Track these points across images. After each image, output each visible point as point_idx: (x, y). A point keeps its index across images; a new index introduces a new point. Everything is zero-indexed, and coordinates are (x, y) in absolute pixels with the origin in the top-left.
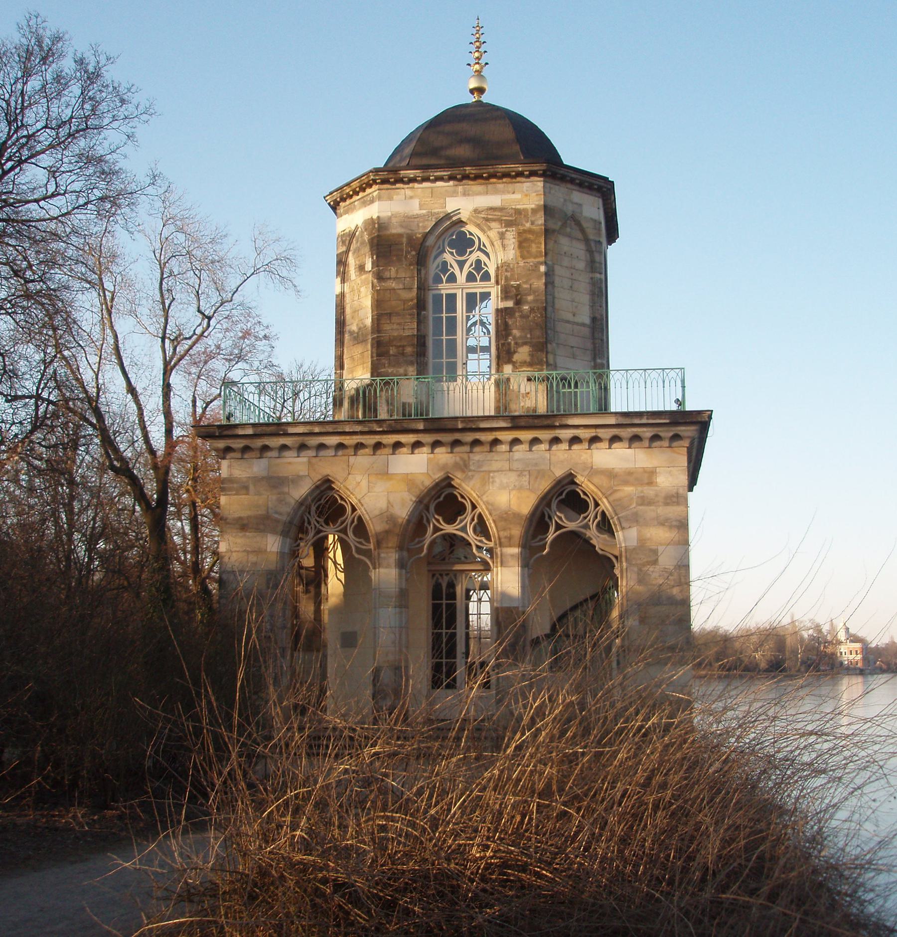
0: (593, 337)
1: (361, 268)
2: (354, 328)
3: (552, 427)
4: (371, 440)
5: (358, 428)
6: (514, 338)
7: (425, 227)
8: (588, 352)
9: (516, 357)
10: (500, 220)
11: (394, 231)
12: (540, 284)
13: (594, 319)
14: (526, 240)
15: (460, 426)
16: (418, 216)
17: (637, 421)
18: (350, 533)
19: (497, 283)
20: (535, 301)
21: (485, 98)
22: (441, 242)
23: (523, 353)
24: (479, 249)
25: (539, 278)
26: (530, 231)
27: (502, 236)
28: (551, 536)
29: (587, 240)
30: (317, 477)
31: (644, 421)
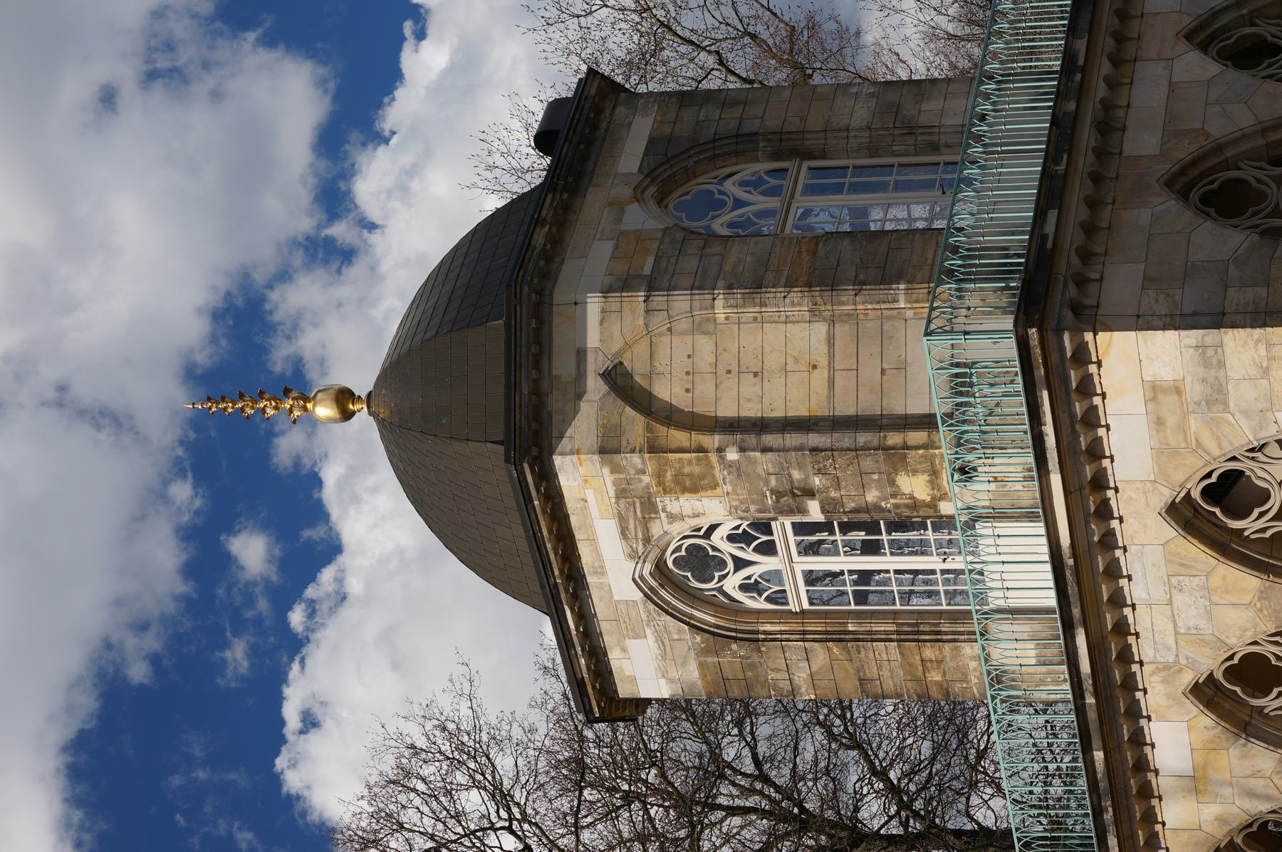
12: (764, 462)
14: (678, 477)
16: (660, 640)
20: (800, 466)
25: (753, 462)
26: (659, 476)
27: (672, 518)
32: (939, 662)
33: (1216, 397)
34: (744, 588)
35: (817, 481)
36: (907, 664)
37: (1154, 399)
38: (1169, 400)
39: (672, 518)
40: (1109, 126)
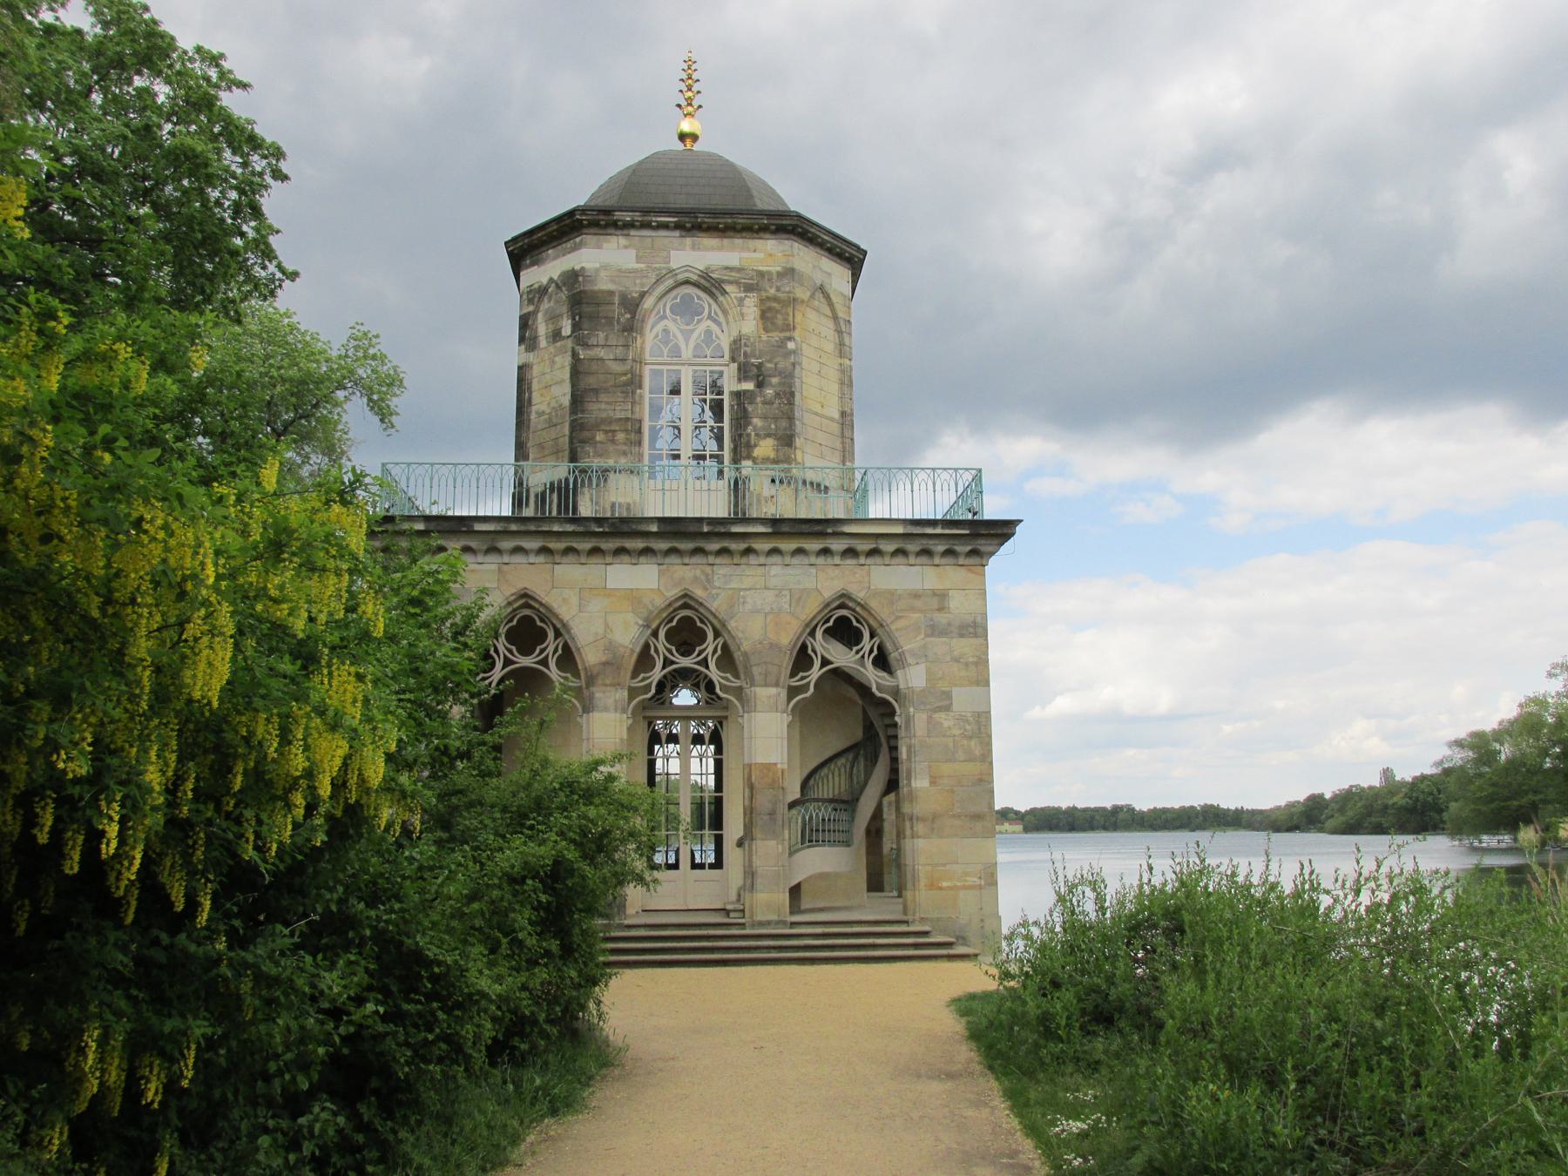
0: (843, 436)
1: (556, 336)
2: (543, 407)
3: (823, 535)
4: (586, 545)
5: (570, 528)
6: (755, 429)
7: (643, 285)
8: (837, 453)
9: (757, 452)
10: (736, 283)
11: (604, 287)
13: (843, 414)
14: (770, 309)
15: (706, 529)
17: (929, 531)
18: (552, 664)
19: (733, 359)
21: (697, 147)
22: (661, 304)
23: (765, 448)
24: (710, 317)
26: (775, 299)
28: (815, 672)
29: (835, 318)
30: (510, 591)
31: (939, 531)
32: (613, 441)
33: (934, 630)
34: (665, 331)
35: (769, 392)
36: (610, 421)
37: (935, 594)
38: (935, 603)
39: (741, 300)
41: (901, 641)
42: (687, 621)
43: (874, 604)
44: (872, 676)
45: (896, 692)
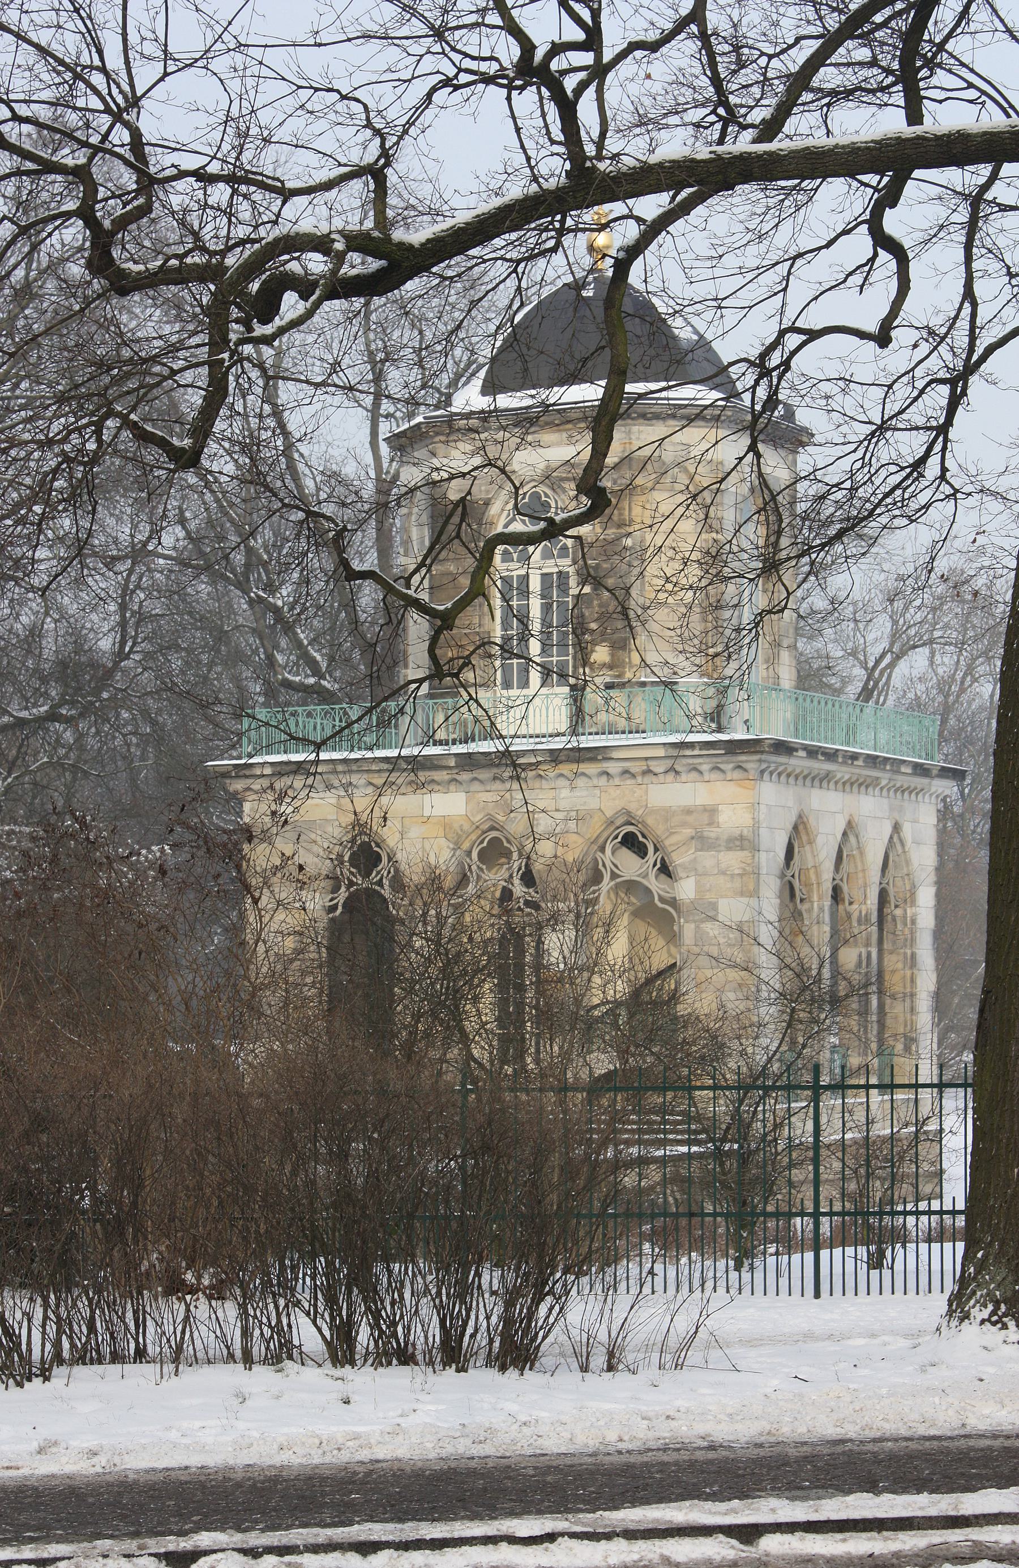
31: (696, 752)
37: (705, 810)
40: (824, 780)
41: (674, 856)
42: (495, 841)
43: (650, 821)
44: (656, 885)
45: (673, 902)
